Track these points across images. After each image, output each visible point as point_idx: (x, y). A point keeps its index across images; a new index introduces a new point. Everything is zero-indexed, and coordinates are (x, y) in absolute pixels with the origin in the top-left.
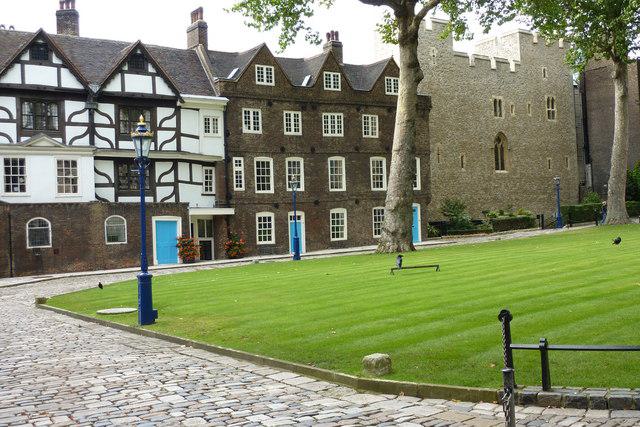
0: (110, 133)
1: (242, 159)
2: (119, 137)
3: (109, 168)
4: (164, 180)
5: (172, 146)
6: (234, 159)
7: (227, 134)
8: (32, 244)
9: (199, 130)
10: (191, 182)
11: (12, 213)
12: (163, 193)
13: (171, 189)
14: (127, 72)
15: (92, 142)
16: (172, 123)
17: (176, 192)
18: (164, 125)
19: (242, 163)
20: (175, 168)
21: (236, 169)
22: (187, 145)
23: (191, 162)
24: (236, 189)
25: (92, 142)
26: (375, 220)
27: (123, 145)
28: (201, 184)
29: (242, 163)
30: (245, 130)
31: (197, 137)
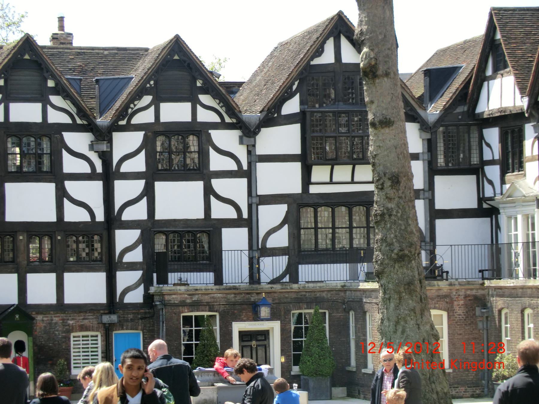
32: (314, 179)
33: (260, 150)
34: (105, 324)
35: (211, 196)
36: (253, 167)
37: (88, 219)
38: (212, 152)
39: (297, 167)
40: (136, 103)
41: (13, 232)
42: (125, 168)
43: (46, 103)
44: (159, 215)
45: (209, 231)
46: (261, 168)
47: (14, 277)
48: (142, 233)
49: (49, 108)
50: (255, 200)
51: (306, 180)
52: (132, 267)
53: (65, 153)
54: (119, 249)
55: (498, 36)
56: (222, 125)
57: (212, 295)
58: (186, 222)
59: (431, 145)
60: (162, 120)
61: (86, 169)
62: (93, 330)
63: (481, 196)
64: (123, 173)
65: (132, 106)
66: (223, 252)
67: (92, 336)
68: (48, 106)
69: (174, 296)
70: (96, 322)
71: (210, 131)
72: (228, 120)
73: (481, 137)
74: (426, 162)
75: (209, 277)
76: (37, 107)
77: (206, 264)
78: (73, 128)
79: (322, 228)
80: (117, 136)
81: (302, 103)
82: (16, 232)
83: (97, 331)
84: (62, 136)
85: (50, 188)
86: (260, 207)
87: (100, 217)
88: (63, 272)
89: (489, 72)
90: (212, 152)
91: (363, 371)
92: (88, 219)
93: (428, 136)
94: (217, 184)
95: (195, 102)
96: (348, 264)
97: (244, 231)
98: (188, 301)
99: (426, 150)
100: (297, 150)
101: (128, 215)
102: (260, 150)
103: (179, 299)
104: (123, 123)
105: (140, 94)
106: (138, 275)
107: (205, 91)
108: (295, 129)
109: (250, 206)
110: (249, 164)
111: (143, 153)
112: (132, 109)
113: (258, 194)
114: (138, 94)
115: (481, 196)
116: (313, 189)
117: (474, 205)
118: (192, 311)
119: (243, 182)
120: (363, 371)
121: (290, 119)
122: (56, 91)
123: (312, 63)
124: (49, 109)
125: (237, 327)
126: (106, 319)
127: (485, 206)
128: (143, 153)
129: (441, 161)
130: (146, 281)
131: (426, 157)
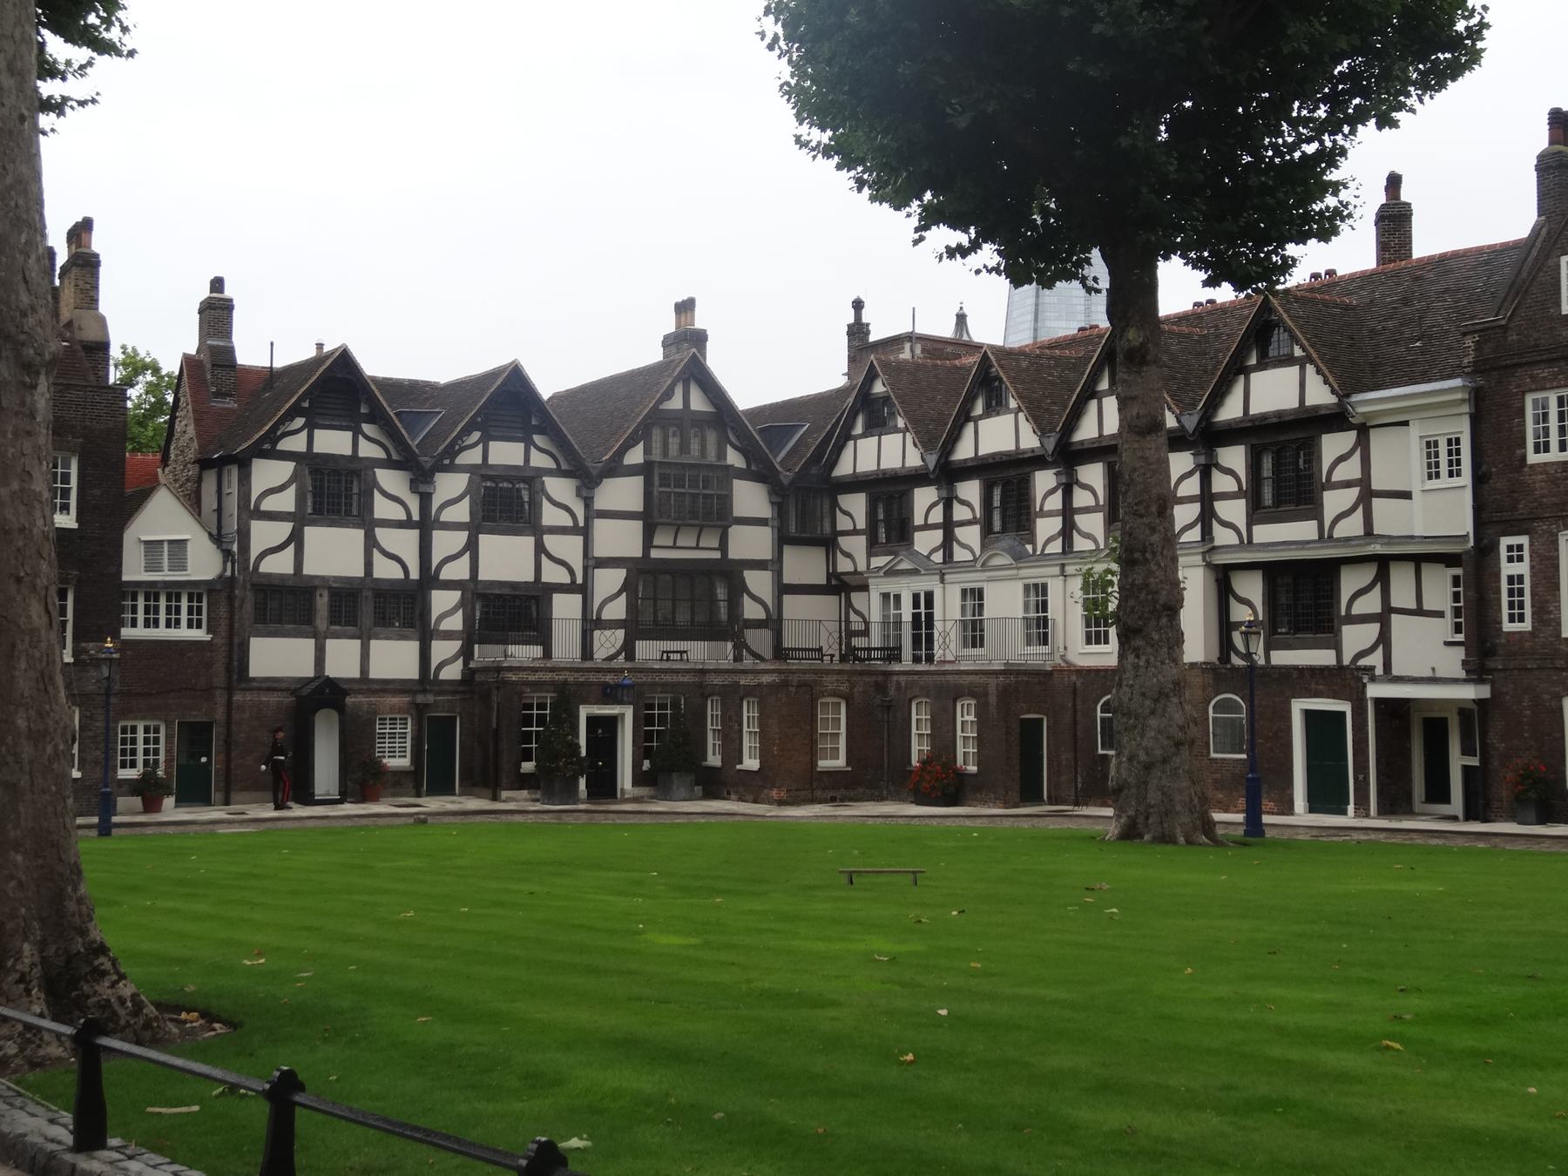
0: (1234, 511)
1: (1524, 540)
2: (1257, 513)
3: (1251, 588)
4: (1359, 608)
5: (1352, 526)
6: (1505, 542)
7: (1479, 480)
8: (1103, 748)
9: (1414, 476)
10: (1420, 612)
11: (1078, 684)
12: (1356, 638)
13: (1373, 630)
14: (1262, 366)
15: (1207, 533)
16: (1350, 470)
17: (1384, 639)
18: (1336, 477)
19: (1526, 553)
20: (1383, 579)
21: (1507, 569)
22: (1390, 518)
23: (1418, 560)
24: (1508, 627)
25: (1207, 533)
26: (124, 752)
27: (1265, 533)
28: (1440, 614)
29: (1526, 553)
30: (1533, 458)
31: (1406, 495)
33: (600, 503)
34: (417, 705)
35: (543, 555)
36: (590, 524)
37: (402, 576)
38: (545, 503)
39: (637, 526)
40: (464, 439)
41: (311, 587)
42: (448, 515)
44: (483, 575)
45: (538, 596)
46: (600, 525)
47: (310, 644)
48: (462, 594)
50: (591, 563)
51: (648, 544)
52: (449, 635)
53: (377, 494)
54: (436, 612)
55: (879, 388)
56: (559, 472)
58: (514, 585)
59: (780, 508)
60: (491, 461)
61: (398, 513)
62: (404, 713)
63: (831, 571)
64: (443, 522)
65: (460, 442)
66: (553, 621)
67: (400, 719)
68: (360, 436)
72: (564, 466)
73: (835, 504)
74: (776, 532)
75: (537, 651)
76: (347, 436)
77: (533, 636)
78: (389, 464)
79: (661, 599)
82: (315, 588)
83: (408, 713)
84: (374, 473)
85: (359, 534)
86: (595, 570)
87: (415, 575)
89: (859, 429)
90: (545, 503)
91: (738, 767)
92: (402, 576)
93: (778, 500)
94: (550, 541)
95: (529, 443)
96: (706, 642)
97: (579, 598)
99: (776, 516)
100: (637, 505)
101: (447, 573)
102: (600, 503)
104: (447, 462)
105: (470, 429)
106: (456, 645)
107: (541, 431)
109: (585, 569)
110: (587, 519)
111: (467, 500)
112: (460, 445)
113: (595, 556)
114: (467, 431)
115: (831, 571)
116: (655, 554)
117: (823, 581)
118: (534, 692)
119: (579, 540)
120: (738, 767)
121: (632, 471)
122: (371, 419)
123: (661, 407)
125: (584, 712)
127: (833, 582)
128: (467, 499)
129: (793, 529)
130: (466, 653)
131: (776, 523)
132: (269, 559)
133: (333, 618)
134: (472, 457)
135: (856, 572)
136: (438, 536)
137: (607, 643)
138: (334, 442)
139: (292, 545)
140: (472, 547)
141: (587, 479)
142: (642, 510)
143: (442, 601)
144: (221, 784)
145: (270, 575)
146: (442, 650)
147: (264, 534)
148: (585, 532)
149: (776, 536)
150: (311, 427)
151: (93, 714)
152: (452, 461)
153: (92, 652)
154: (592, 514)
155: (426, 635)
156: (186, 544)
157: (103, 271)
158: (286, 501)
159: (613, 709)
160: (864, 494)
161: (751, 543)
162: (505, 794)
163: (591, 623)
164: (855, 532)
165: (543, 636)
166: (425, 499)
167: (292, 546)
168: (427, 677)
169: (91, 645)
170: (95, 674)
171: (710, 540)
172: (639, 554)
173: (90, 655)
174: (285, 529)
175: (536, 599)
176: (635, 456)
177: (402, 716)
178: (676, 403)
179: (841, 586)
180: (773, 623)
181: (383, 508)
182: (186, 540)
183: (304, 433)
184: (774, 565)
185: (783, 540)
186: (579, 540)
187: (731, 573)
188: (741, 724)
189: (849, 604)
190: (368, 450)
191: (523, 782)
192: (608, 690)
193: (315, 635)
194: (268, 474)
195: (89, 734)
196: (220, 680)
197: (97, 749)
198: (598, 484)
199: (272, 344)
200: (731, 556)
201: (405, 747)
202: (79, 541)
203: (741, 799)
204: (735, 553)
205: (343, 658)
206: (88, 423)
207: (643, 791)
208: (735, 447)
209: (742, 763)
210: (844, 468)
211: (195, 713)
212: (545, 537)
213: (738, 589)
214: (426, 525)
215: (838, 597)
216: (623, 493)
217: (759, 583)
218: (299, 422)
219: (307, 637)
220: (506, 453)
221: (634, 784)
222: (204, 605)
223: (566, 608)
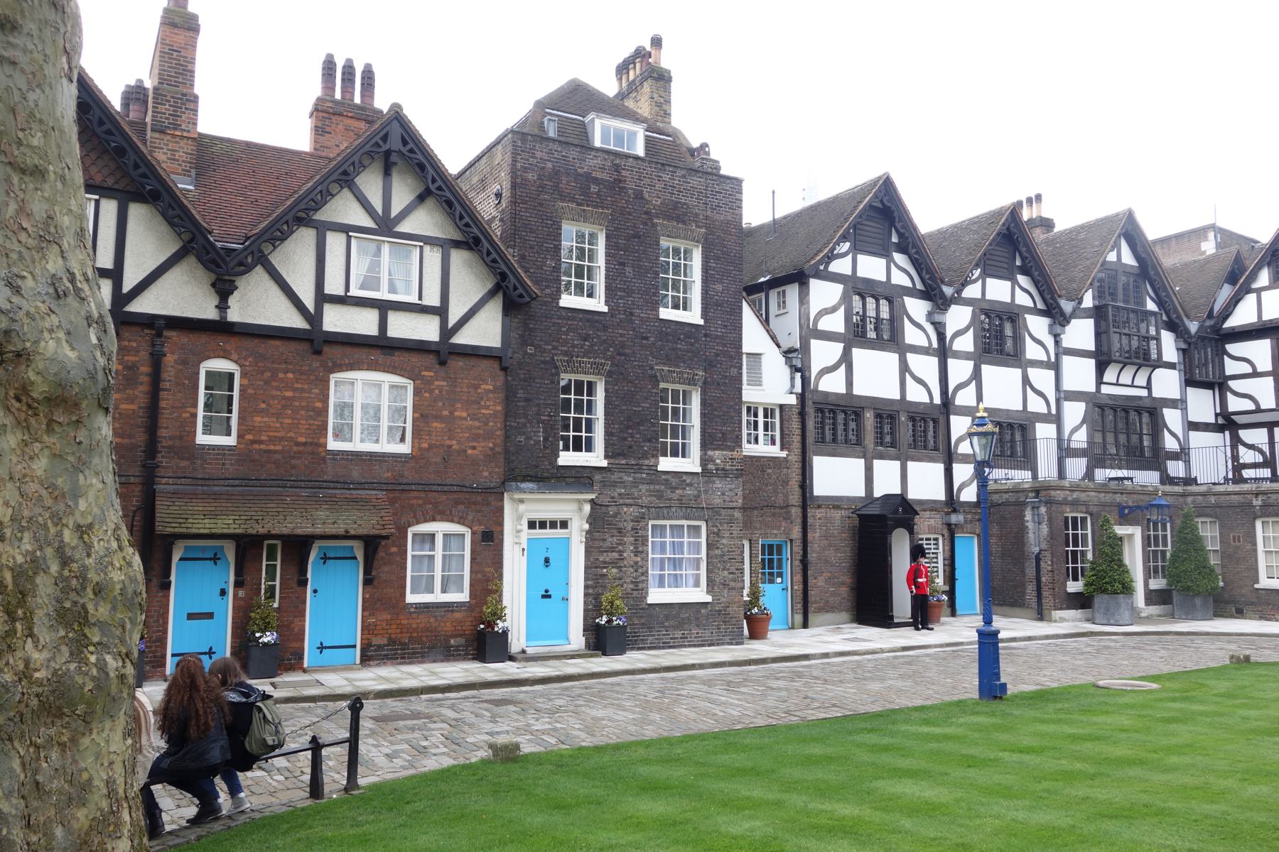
32: (1105, 379)
37: (927, 401)
38: (1028, 338)
39: (1091, 363)
43: (890, 260)
46: (1067, 361)
49: (893, 266)
50: (1062, 395)
51: (1100, 381)
52: (965, 459)
57: (1088, 493)
63: (1218, 411)
65: (970, 275)
69: (1058, 492)
70: (940, 523)
71: (1026, 316)
72: (1040, 305)
76: (882, 262)
80: (954, 309)
81: (1094, 298)
84: (903, 300)
87: (937, 400)
88: (907, 460)
92: (927, 401)
94: (1033, 373)
97: (1053, 427)
98: (1070, 499)
99: (1182, 360)
100: (1090, 345)
103: (1062, 496)
107: (1025, 271)
108: (1090, 323)
109: (1058, 401)
110: (1057, 355)
111: (971, 332)
116: (1105, 389)
119: (1052, 373)
120: (1256, 586)
121: (1087, 314)
124: (893, 269)
126: (954, 518)
127: (1220, 421)
131: (1182, 367)
132: (826, 377)
133: (880, 441)
134: (972, 291)
135: (1259, 410)
136: (951, 362)
137: (1076, 468)
138: (871, 267)
139: (843, 366)
140: (977, 376)
141: (1058, 317)
142: (1094, 349)
143: (960, 425)
144: (799, 606)
145: (826, 394)
146: (963, 472)
147: (823, 354)
148: (1056, 367)
149: (1183, 379)
150: (856, 249)
151: (719, 530)
152: (959, 292)
153: (718, 461)
154: (1061, 351)
155: (949, 459)
156: (760, 358)
157: (674, 86)
158: (835, 323)
159: (1127, 530)
160: (1269, 340)
161: (1167, 383)
162: (1057, 614)
163: (1065, 451)
164: (1255, 374)
165: (1028, 460)
166: (940, 329)
167: (843, 367)
168: (951, 502)
169: (717, 453)
170: (720, 486)
171: (1141, 380)
172: (1092, 388)
173: (717, 464)
174: (837, 349)
175: (1023, 428)
176: (1088, 301)
177: (936, 536)
178: (1112, 257)
179: (1227, 424)
180: (1183, 454)
181: (912, 336)
182: (760, 354)
183: (850, 256)
184: (1179, 404)
185: (1190, 382)
186: (1052, 373)
187: (1152, 410)
188: (1255, 544)
189: (1236, 441)
190: (899, 279)
191: (1082, 602)
192: (1126, 511)
193: (864, 457)
194: (823, 294)
195: (718, 552)
196: (795, 498)
197: (724, 569)
198: (1068, 322)
199: (774, 192)
200: (1154, 395)
201: (937, 567)
202: (704, 339)
203: (1263, 617)
204: (1156, 394)
205: (887, 478)
206: (709, 213)
207: (1154, 610)
208: (1152, 298)
209: (1258, 582)
210: (1244, 315)
211: (775, 532)
212: (1029, 370)
213: (1158, 425)
214: (943, 352)
215: (1222, 435)
216: (1081, 333)
217: (1172, 418)
218: (847, 245)
219: (858, 457)
220: (998, 290)
221: (1149, 601)
222: (777, 421)
223: (1045, 432)
